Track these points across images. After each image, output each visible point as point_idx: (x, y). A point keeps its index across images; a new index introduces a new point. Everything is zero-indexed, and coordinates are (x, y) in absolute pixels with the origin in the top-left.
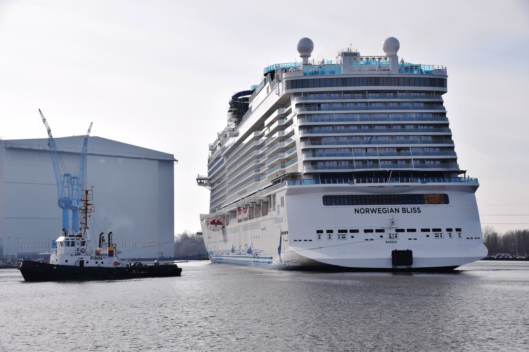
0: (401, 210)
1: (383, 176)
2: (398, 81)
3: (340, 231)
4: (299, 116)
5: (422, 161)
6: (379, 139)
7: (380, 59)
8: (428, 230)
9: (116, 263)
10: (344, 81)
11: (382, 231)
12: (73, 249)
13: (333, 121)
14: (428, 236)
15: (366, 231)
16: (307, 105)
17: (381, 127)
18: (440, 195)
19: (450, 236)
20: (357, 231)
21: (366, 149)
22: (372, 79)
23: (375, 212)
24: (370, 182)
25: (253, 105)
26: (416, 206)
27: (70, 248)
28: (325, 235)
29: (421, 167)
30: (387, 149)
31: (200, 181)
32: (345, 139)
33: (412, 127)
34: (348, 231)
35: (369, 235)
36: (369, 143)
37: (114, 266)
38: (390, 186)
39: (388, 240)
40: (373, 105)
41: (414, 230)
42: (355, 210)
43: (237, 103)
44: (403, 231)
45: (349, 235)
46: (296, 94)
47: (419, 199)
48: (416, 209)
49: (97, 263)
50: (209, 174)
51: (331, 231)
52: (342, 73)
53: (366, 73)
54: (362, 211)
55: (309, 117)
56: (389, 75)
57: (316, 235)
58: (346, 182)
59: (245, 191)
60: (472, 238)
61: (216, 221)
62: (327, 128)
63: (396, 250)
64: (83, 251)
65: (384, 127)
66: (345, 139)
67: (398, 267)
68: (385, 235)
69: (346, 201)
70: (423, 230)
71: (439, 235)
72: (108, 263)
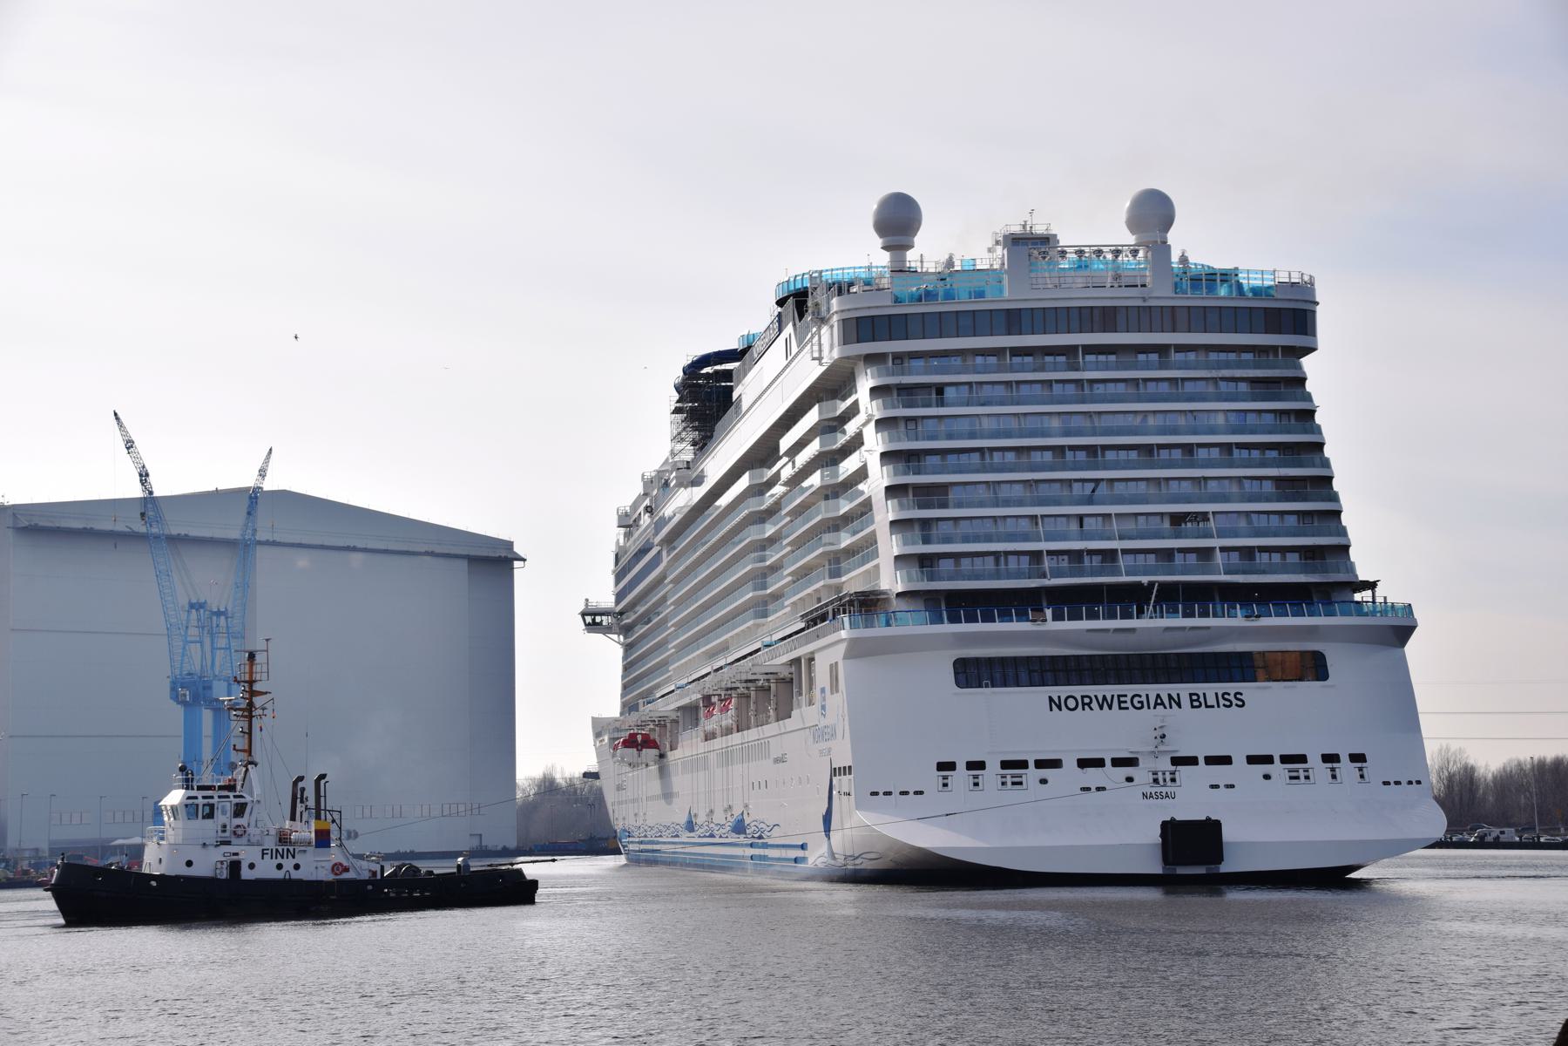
0: (1185, 701)
1: (1130, 598)
2: (1170, 318)
3: (1006, 765)
4: (881, 424)
5: (1248, 553)
6: (1119, 488)
7: (1117, 253)
8: (1268, 760)
9: (338, 868)
10: (1013, 320)
11: (1131, 762)
12: (209, 828)
13: (982, 437)
14: (1267, 777)
15: (1083, 763)
16: (904, 390)
17: (1123, 454)
18: (1303, 653)
19: (1334, 777)
20: (1055, 764)
21: (1081, 518)
22: (1096, 312)
23: (1110, 707)
24: (1093, 616)
25: (745, 391)
26: (1231, 687)
27: (200, 823)
28: (961, 776)
29: (1244, 572)
30: (1141, 519)
31: (593, 620)
32: (1018, 491)
33: (1215, 452)
34: (1031, 764)
35: (1093, 776)
36: (1090, 501)
37: (331, 877)
38: (1152, 628)
39: (1148, 790)
40: (1100, 389)
41: (1226, 760)
42: (1051, 699)
43: (700, 386)
45: (1032, 774)
46: (871, 359)
47: (1239, 667)
48: (1231, 697)
49: (280, 867)
50: (619, 597)
51: (980, 765)
52: (1006, 294)
53: (1079, 296)
54: (1071, 703)
55: (911, 425)
56: (1144, 299)
57: (936, 776)
58: (1022, 616)
59: (724, 648)
60: (1398, 783)
61: (639, 738)
62: (964, 457)
63: (1173, 820)
64: (239, 831)
65: (1133, 455)
66: (1018, 491)
67: (1181, 870)
68: (1141, 774)
69: (1024, 676)
70: (1252, 760)
71: (1302, 774)
72: (314, 867)
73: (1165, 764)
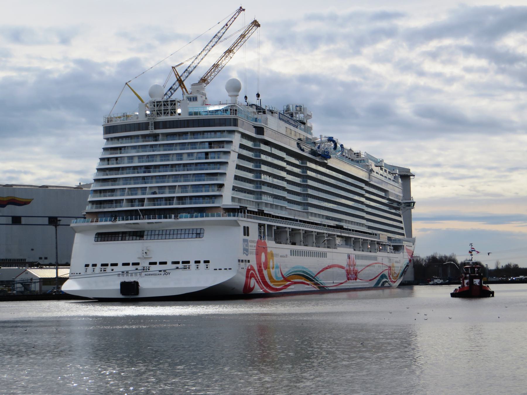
8: (178, 263)
14: (177, 268)
15: (124, 264)
20: (116, 265)
28: (90, 268)
34: (109, 265)
35: (126, 268)
41: (165, 263)
44: (155, 263)
45: (109, 268)
57: (84, 268)
68: (139, 267)
70: (174, 263)
73: (147, 265)
